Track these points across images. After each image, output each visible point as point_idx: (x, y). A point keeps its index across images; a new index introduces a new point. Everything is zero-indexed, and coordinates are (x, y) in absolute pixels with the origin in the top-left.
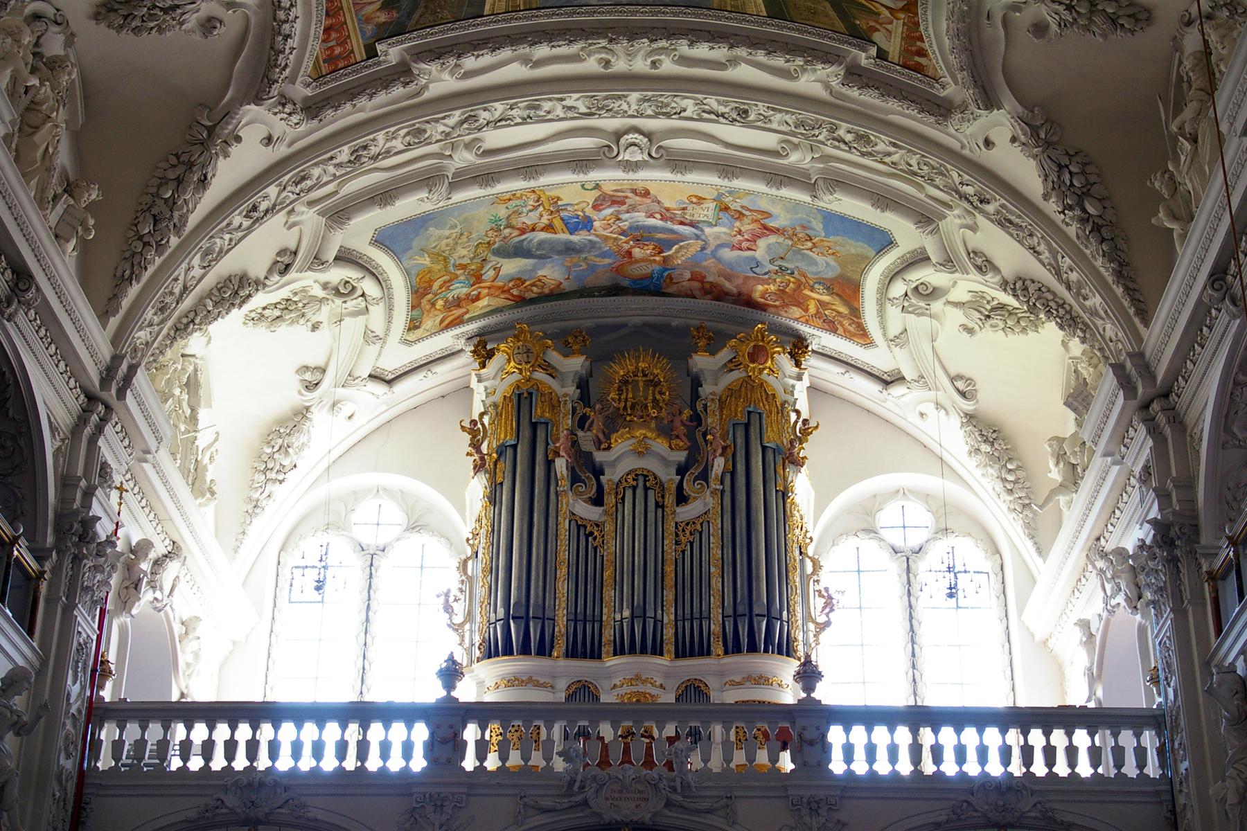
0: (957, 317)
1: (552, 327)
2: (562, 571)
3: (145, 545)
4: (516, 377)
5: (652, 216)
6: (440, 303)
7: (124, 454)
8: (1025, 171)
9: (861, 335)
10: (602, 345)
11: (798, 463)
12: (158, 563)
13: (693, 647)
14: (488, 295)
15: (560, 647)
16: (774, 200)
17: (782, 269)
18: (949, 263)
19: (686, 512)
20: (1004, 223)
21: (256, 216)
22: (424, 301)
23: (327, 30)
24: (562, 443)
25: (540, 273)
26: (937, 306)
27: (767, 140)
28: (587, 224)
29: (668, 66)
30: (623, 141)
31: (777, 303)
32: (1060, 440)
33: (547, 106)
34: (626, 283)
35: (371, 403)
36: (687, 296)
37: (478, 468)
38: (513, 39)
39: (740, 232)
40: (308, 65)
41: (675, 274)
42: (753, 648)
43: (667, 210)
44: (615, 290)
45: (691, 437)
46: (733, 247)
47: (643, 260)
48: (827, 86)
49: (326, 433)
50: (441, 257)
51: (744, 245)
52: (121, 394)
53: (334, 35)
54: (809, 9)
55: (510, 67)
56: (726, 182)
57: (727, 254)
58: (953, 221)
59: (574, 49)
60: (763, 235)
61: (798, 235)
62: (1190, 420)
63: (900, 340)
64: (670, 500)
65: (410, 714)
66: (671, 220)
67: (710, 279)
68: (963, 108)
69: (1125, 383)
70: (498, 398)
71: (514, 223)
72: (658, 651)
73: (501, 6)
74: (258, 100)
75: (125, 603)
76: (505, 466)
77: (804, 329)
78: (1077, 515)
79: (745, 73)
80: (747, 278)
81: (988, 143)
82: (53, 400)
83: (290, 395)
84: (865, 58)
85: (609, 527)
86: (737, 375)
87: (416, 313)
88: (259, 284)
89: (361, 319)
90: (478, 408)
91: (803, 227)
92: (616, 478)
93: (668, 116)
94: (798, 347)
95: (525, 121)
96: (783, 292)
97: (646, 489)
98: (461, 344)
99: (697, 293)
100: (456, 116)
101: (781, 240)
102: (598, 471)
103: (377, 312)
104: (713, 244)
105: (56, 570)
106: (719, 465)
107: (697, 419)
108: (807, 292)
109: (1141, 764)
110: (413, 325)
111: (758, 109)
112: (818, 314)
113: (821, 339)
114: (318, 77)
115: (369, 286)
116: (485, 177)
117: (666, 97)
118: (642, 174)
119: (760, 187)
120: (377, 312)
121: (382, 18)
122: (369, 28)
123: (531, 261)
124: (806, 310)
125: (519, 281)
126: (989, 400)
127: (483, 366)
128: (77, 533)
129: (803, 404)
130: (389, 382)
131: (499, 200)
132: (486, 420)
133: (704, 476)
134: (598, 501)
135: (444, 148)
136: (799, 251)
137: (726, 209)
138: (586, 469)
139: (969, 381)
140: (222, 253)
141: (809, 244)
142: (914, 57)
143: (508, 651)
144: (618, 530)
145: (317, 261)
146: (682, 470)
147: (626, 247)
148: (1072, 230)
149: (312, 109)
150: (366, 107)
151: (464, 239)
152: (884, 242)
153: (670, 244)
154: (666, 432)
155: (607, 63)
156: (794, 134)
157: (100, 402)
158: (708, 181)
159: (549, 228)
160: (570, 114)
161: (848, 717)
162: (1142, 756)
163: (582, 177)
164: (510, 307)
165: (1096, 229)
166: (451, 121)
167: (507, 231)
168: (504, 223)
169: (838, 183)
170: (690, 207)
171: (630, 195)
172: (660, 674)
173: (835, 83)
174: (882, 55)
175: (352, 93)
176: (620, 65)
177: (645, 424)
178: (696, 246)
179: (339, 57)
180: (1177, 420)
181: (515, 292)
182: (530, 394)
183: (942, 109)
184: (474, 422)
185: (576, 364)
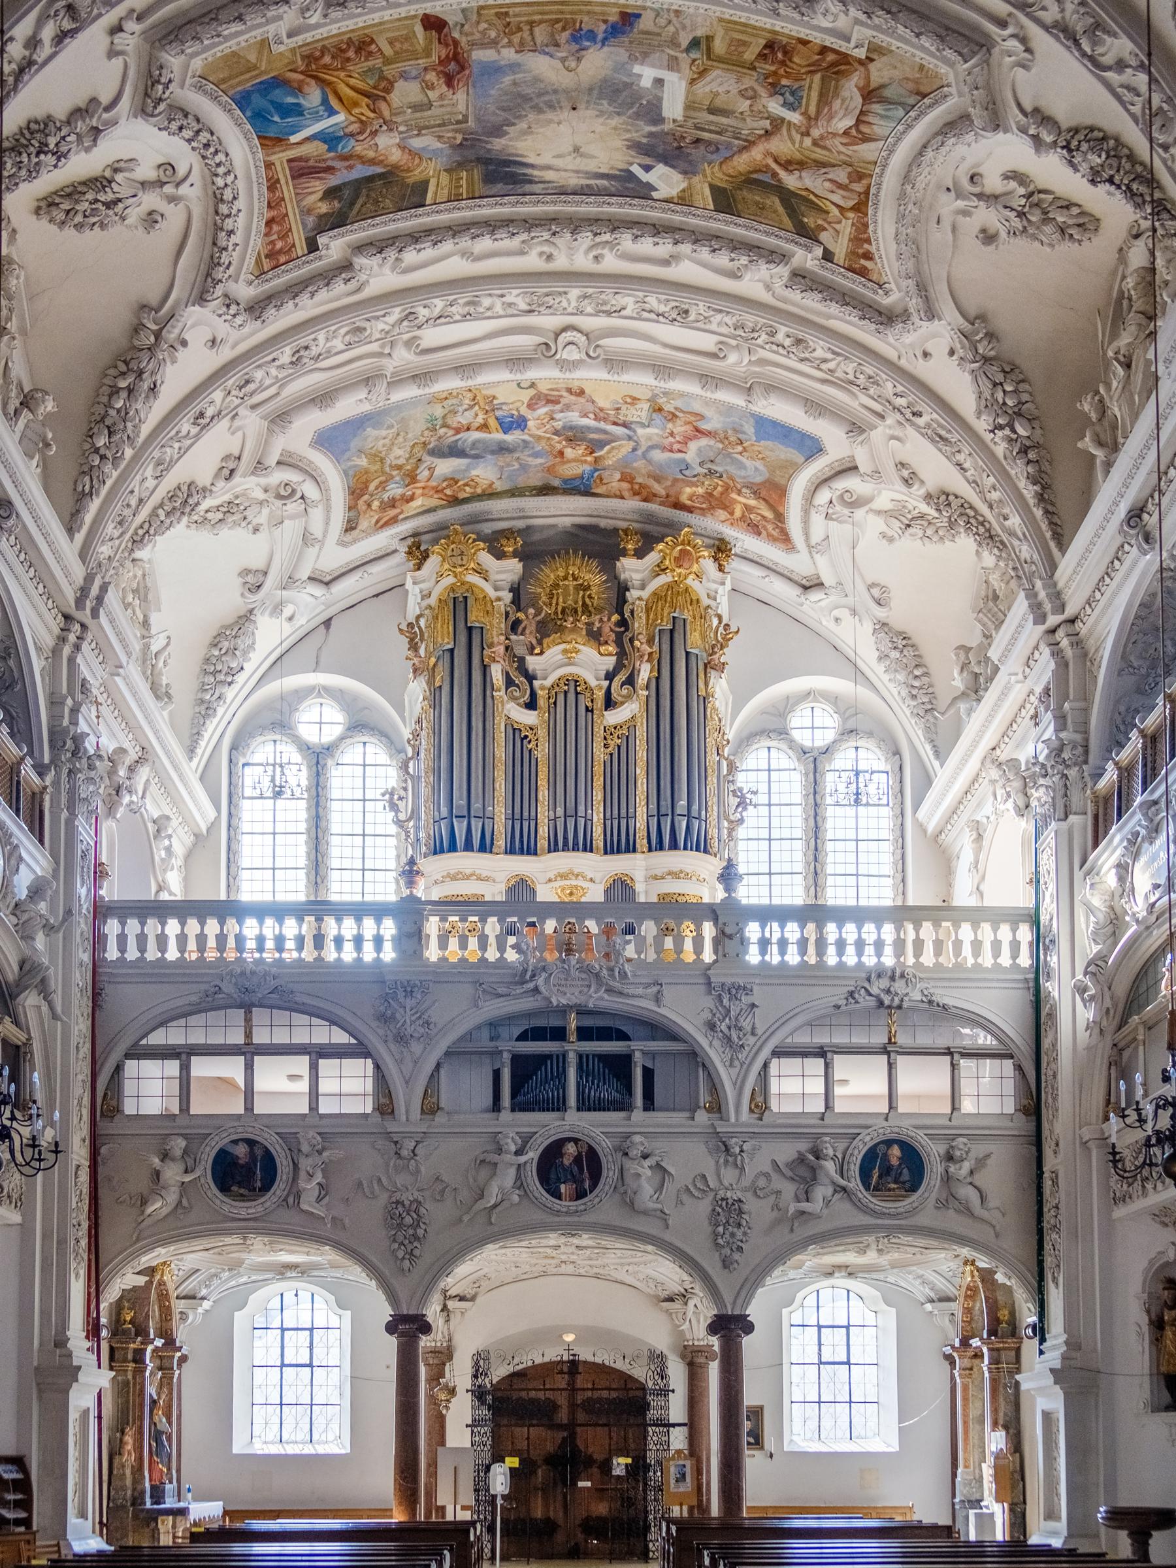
1: (488, 528)
5: (585, 416)
9: (784, 539)
16: (707, 403)
17: (711, 472)
22: (361, 502)
23: (269, 223)
25: (474, 473)
27: (707, 342)
28: (520, 423)
29: (611, 263)
30: (561, 339)
33: (486, 302)
34: (556, 483)
36: (616, 496)
38: (455, 230)
39: (672, 434)
41: (605, 474)
43: (601, 410)
44: (545, 490)
46: (663, 449)
47: (574, 460)
50: (377, 458)
51: (676, 447)
53: (275, 228)
54: (757, 203)
56: (662, 384)
57: (658, 456)
59: (516, 242)
60: (695, 437)
61: (731, 439)
66: (605, 420)
67: (639, 480)
71: (449, 421)
73: (444, 194)
80: (676, 480)
87: (352, 514)
90: (413, 608)
91: (735, 430)
93: (609, 313)
94: (721, 549)
95: (466, 317)
96: (711, 495)
98: (395, 544)
99: (626, 494)
100: (396, 314)
101: (712, 442)
104: (644, 445)
108: (734, 496)
110: (350, 527)
111: (699, 307)
112: (743, 518)
113: (743, 541)
115: (310, 489)
116: (421, 377)
117: (608, 295)
118: (578, 374)
119: (693, 388)
120: (317, 514)
121: (324, 208)
122: (311, 220)
123: (463, 462)
124: (732, 514)
127: (419, 567)
131: (434, 400)
135: (383, 346)
136: (729, 455)
137: (660, 410)
141: (740, 448)
147: (559, 447)
150: (308, 306)
151: (401, 439)
153: (601, 444)
155: (550, 257)
156: (734, 337)
158: (643, 381)
159: (484, 427)
160: (510, 311)
163: (519, 377)
164: (443, 507)
166: (391, 319)
167: (443, 430)
168: (439, 422)
169: (771, 388)
170: (624, 407)
171: (565, 394)
174: (828, 256)
176: (561, 262)
178: (628, 446)
179: (280, 252)
181: (448, 492)
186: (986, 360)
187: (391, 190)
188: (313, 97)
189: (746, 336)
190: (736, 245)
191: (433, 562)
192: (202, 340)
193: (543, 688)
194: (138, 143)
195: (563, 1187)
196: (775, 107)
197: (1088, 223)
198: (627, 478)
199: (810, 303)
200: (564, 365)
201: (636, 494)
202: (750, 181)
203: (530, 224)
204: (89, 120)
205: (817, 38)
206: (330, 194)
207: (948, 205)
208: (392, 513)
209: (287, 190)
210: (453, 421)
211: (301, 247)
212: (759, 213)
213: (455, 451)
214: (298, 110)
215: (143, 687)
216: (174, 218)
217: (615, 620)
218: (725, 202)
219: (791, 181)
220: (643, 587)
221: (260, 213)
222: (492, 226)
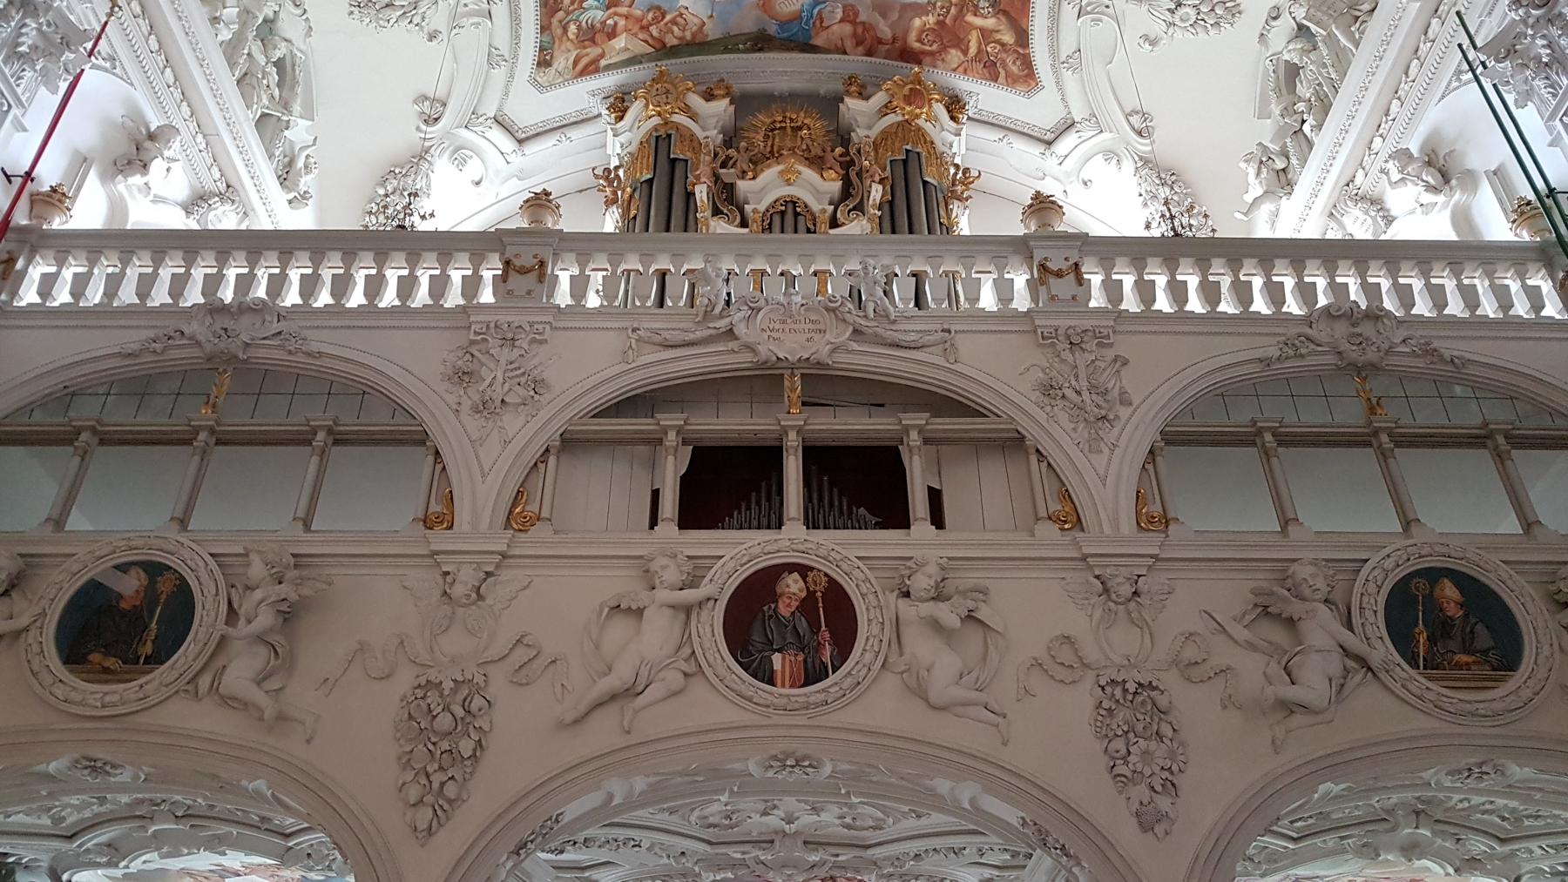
4: (656, 120)
6: (573, 28)
14: (627, 30)
22: (555, 21)
31: (935, 47)
37: (610, 202)
67: (863, 17)
70: (633, 148)
86: (892, 119)
92: (762, 207)
94: (955, 106)
97: (797, 214)
99: (849, 44)
106: (877, 193)
108: (970, 18)
112: (978, 57)
124: (965, 52)
132: (621, 173)
133: (860, 208)
134: (744, 224)
139: (1145, 116)
154: (817, 163)
182: (669, 136)
184: (607, 170)
193: (755, 211)
195: (777, 659)
208: (593, 52)
220: (870, 128)
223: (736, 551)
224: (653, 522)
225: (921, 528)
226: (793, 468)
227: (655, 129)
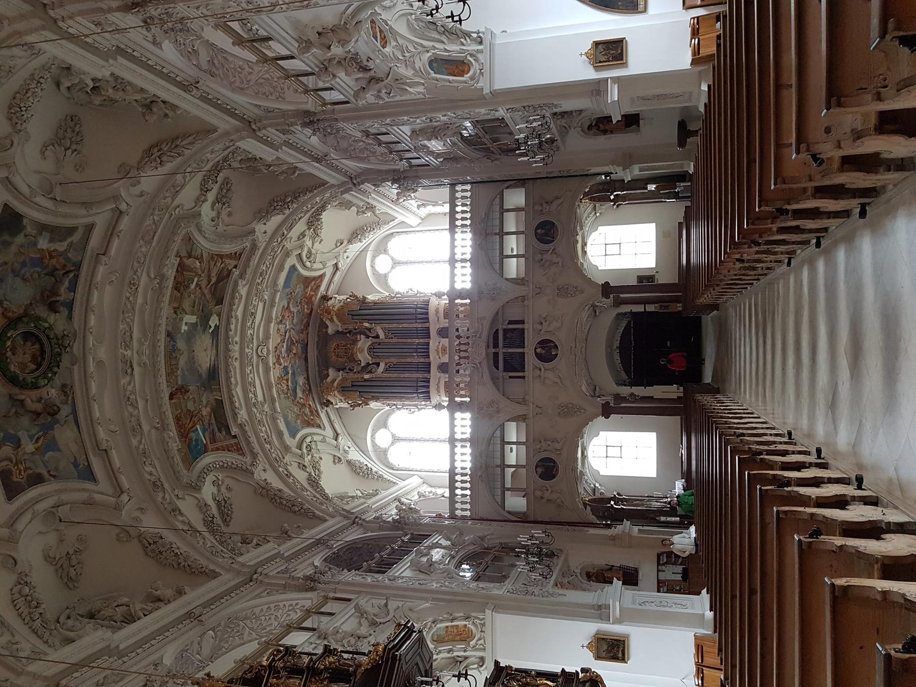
0: (317, 244)
1: (318, 380)
2: (402, 376)
3: (397, 507)
7: (370, 513)
8: (276, 220)
9: (322, 277)
10: (324, 364)
11: (364, 298)
12: (402, 504)
13: (427, 333)
15: (426, 375)
18: (301, 247)
19: (382, 335)
20: (291, 228)
21: (289, 475)
24: (359, 376)
26: (313, 251)
27: (261, 305)
28: (285, 368)
29: (237, 339)
32: (358, 212)
35: (343, 441)
37: (367, 404)
40: (240, 457)
42: (427, 313)
44: (306, 359)
45: (356, 334)
48: (245, 285)
49: (354, 455)
52: (353, 513)
55: (238, 391)
58: (288, 245)
61: (290, 297)
62: (359, 171)
63: (324, 264)
64: (377, 340)
65: (452, 419)
68: (254, 240)
69: (347, 191)
70: (343, 398)
72: (428, 344)
74: (253, 473)
75: (417, 511)
76: (366, 395)
77: (319, 296)
78: (383, 207)
79: (239, 313)
81: (265, 232)
82: (354, 535)
83: (343, 467)
84: (236, 272)
85: (387, 360)
86: (335, 319)
88: (310, 475)
89: (318, 443)
90: (345, 405)
94: (325, 298)
95: (255, 387)
102: (368, 365)
103: (316, 438)
105: (410, 529)
106: (366, 325)
107: (350, 332)
109: (467, 191)
110: (319, 427)
114: (243, 454)
115: (308, 440)
116: (273, 401)
120: (316, 438)
122: (228, 437)
125: (304, 391)
126: (344, 235)
128: (398, 524)
129: (344, 297)
130: (338, 434)
133: (369, 329)
134: (378, 364)
138: (367, 368)
140: (302, 485)
142: (237, 256)
143: (428, 392)
144: (388, 357)
145: (302, 456)
146: (368, 337)
148: (295, 206)
149: (254, 456)
150: (253, 439)
152: (293, 267)
154: (355, 342)
157: (355, 520)
161: (453, 282)
162: (464, 191)
165: (296, 198)
169: (275, 284)
172: (435, 343)
173: (244, 283)
174: (235, 267)
175: (249, 443)
176: (237, 355)
177: (353, 349)
180: (359, 175)
183: (254, 247)
185: (331, 371)
186: (267, 213)
187: (218, 410)
188: (193, 435)
189: (259, 293)
190: (233, 297)
191: (330, 398)
192: (265, 475)
194: (208, 491)
196: (193, 286)
197: (227, 181)
198: (303, 330)
199: (249, 271)
200: (268, 353)
201: (307, 329)
202: (213, 293)
203: (227, 366)
204: (203, 507)
205: (174, 274)
206: (220, 432)
207: (221, 228)
209: (219, 444)
210: (286, 391)
211: (235, 441)
212: (223, 290)
213: (295, 390)
214: (197, 440)
215: (374, 499)
216: (228, 481)
217: (349, 336)
218: (220, 302)
219: (214, 280)
221: (225, 453)
222: (228, 378)
223: (531, 360)
224: (523, 377)
225: (526, 326)
226: (521, 350)
227: (339, 392)
